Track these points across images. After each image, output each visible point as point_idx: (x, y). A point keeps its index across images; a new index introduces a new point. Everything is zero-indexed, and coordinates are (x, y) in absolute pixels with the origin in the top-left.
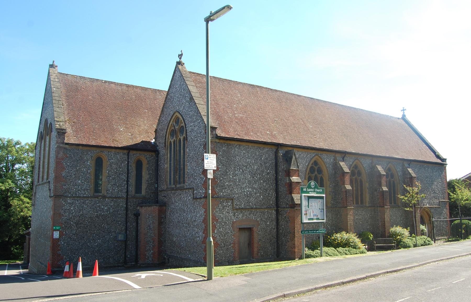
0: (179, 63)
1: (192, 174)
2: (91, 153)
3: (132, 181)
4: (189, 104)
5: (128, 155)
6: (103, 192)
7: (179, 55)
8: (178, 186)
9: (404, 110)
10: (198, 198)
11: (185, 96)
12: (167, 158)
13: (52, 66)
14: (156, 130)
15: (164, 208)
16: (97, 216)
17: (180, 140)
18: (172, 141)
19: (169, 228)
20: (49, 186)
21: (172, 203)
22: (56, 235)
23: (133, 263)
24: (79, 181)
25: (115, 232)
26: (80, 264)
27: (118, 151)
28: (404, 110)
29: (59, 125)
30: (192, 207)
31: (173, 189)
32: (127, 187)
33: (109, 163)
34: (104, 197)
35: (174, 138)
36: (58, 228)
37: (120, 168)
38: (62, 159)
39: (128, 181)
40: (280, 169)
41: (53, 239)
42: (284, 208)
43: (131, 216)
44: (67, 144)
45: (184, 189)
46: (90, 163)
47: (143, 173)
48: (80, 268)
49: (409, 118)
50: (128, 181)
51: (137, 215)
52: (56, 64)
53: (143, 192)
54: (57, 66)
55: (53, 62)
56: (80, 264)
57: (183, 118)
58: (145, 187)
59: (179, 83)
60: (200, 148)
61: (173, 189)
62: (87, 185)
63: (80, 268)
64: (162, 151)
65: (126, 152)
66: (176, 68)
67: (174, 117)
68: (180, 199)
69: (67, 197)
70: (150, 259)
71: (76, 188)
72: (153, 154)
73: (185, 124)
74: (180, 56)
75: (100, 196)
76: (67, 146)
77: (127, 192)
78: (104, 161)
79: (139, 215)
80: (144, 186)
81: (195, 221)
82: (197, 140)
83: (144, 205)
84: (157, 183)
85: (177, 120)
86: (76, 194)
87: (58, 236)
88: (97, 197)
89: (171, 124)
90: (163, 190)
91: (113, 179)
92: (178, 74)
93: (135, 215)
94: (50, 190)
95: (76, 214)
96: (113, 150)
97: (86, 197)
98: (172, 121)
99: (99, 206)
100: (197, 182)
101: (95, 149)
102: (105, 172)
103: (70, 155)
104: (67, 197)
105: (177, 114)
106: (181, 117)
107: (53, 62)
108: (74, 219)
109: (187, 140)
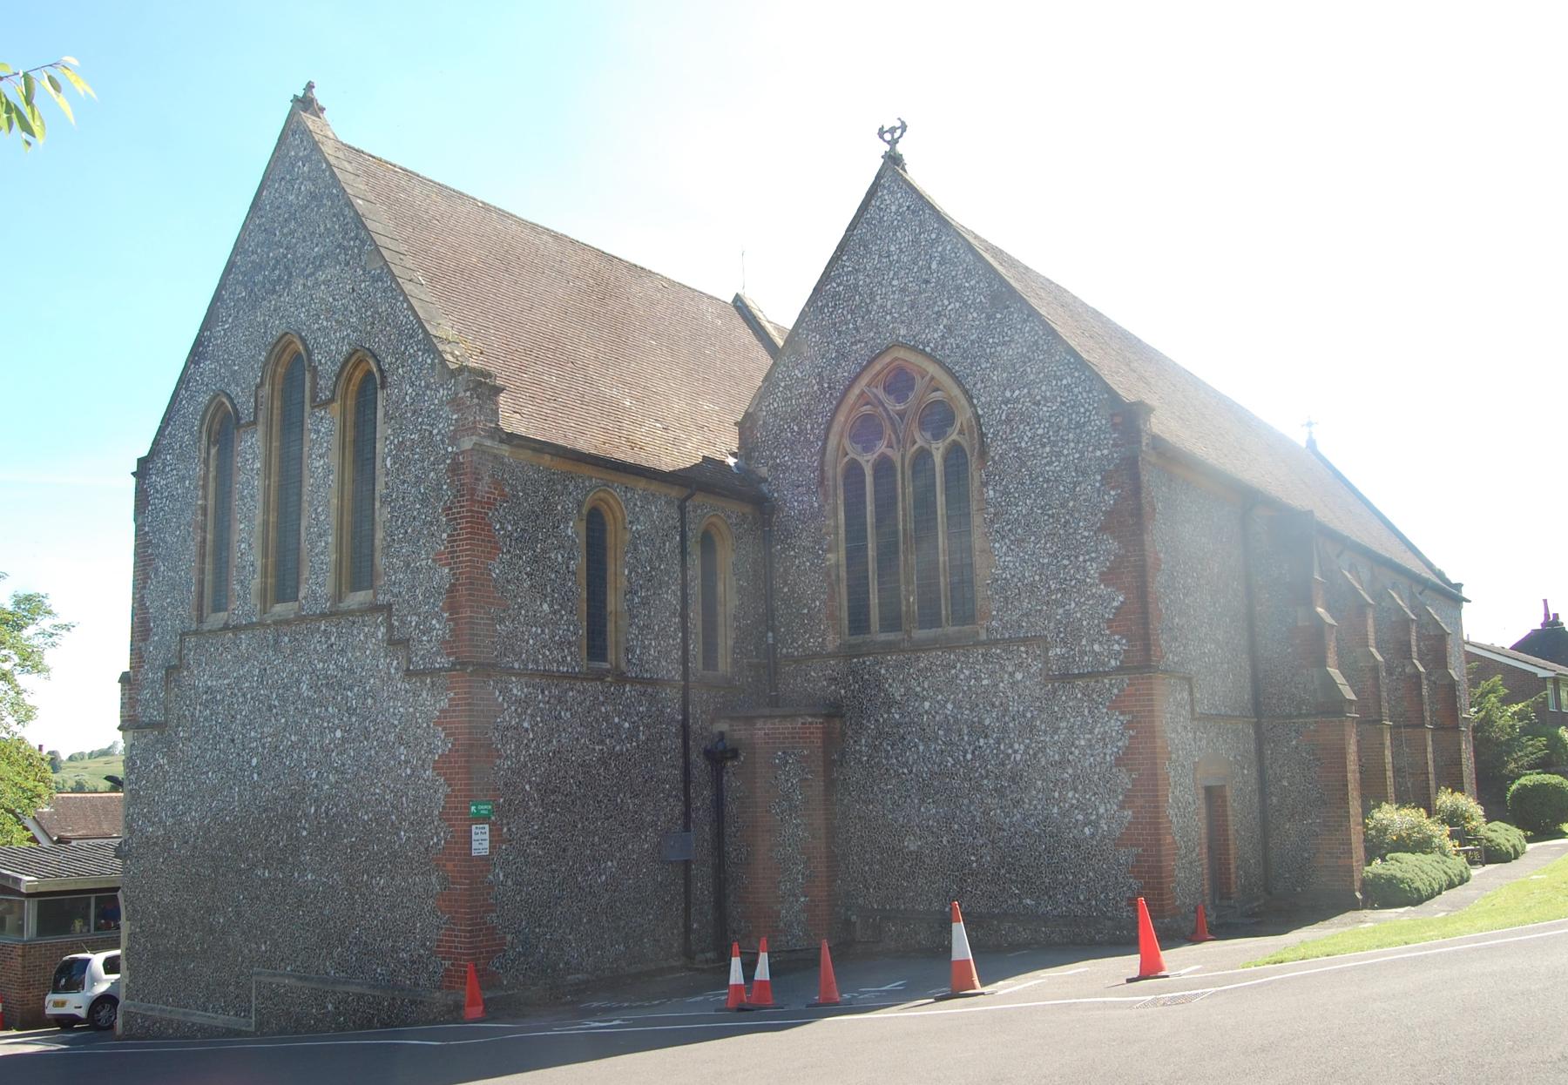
0: (893, 161)
2: (576, 487)
4: (989, 318)
5: (682, 509)
6: (611, 656)
7: (881, 133)
8: (919, 634)
9: (1310, 424)
10: (1080, 676)
12: (836, 527)
13: (306, 102)
14: (747, 415)
15: (837, 723)
16: (603, 762)
17: (924, 456)
18: (867, 461)
19: (867, 802)
20: (390, 627)
21: (889, 703)
22: (481, 841)
23: (710, 955)
24: (545, 606)
25: (654, 824)
26: (959, 931)
27: (654, 487)
28: (1310, 424)
29: (452, 354)
30: (1041, 710)
31: (889, 647)
32: (685, 640)
33: (628, 536)
34: (621, 678)
35: (881, 448)
36: (484, 809)
38: (490, 504)
39: (684, 616)
41: (473, 859)
42: (1289, 716)
43: (699, 762)
44: (511, 438)
45: (983, 644)
46: (574, 530)
47: (720, 587)
48: (961, 946)
49: (1321, 449)
52: (319, 95)
53: (724, 664)
54: (322, 110)
56: (959, 931)
57: (949, 371)
58: (730, 643)
59: (904, 236)
60: (1076, 484)
61: (889, 647)
62: (569, 623)
63: (961, 946)
64: (794, 501)
65: (675, 493)
66: (879, 177)
67: (877, 367)
69: (510, 671)
70: (797, 931)
71: (537, 635)
72: (748, 509)
73: (966, 392)
74: (892, 135)
75: (608, 671)
76: (505, 450)
77: (685, 660)
78: (610, 528)
79: (734, 754)
80: (726, 640)
81: (1061, 764)
82: (1059, 454)
83: (767, 711)
85: (899, 382)
86: (536, 662)
87: (486, 844)
88: (600, 677)
89: (856, 391)
90: (815, 655)
92: (892, 202)
93: (709, 754)
94: (397, 643)
95: (537, 748)
96: (642, 484)
97: (564, 676)
98: (864, 381)
99: (607, 718)
100: (1067, 614)
101: (587, 470)
103: (513, 487)
104: (510, 671)
105: (901, 353)
106: (932, 369)
108: (534, 770)
109: (983, 453)
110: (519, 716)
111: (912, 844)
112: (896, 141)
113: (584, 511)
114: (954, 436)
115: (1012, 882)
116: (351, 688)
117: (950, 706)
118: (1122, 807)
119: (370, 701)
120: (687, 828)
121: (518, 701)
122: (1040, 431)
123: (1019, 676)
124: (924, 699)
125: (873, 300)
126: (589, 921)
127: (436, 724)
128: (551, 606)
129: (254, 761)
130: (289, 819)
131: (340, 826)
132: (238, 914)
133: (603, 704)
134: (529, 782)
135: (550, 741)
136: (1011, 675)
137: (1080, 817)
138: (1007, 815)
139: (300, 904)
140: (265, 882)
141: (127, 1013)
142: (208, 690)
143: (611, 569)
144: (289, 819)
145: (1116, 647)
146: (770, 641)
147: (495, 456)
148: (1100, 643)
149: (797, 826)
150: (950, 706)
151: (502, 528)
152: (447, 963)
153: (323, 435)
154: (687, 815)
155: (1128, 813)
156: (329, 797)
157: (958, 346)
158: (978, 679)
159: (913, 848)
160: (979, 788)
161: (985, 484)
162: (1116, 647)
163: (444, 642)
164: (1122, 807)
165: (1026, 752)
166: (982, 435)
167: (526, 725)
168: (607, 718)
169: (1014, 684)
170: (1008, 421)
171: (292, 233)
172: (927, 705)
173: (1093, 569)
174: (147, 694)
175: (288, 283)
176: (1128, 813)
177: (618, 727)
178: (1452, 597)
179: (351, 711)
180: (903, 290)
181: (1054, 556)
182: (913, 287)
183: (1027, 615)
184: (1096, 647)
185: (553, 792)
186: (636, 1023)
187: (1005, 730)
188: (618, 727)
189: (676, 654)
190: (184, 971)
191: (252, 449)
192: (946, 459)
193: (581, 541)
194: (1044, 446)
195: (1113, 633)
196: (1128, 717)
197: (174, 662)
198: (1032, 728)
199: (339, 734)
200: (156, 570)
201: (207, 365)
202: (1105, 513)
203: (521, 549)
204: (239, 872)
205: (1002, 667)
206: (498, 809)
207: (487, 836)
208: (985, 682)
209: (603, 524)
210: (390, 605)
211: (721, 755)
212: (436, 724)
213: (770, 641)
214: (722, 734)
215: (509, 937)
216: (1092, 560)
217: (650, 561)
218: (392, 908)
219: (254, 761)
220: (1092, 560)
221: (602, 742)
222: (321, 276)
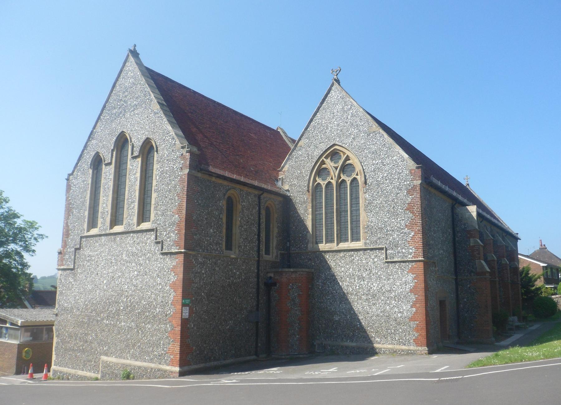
1: (381, 228)
3: (263, 235)
11: (357, 125)
24: (211, 230)
37: (252, 215)
39: (259, 236)
40: (458, 229)
43: (262, 286)
46: (223, 203)
50: (259, 236)
51: (270, 285)
55: (135, 46)
60: (398, 194)
65: (257, 192)
68: (352, 261)
71: (208, 241)
79: (274, 284)
84: (289, 241)
87: (187, 314)
91: (246, 230)
93: (266, 284)
99: (231, 270)
102: (237, 220)
107: (135, 46)
108: (205, 288)
109: (366, 183)
110: (201, 268)
111: (337, 318)
112: (337, 75)
113: (226, 197)
114: (355, 176)
115: (372, 332)
116: (141, 257)
117: (351, 270)
118: (412, 307)
119: (147, 262)
120: (257, 310)
121: (201, 263)
122: (385, 175)
123: (376, 260)
124: (342, 267)
125: (327, 128)
126: (223, 342)
127: (171, 271)
128: (213, 230)
129: (105, 282)
130: (116, 303)
131: (134, 306)
132: (96, 335)
133: (230, 265)
134: (203, 292)
135: (211, 278)
136: (373, 259)
137: (397, 310)
138: (370, 308)
139: (119, 333)
140: (107, 325)
141: (54, 370)
142: (89, 256)
143: (234, 218)
144: (116, 303)
145: (411, 251)
146: (288, 245)
147: (196, 177)
148: (405, 249)
149: (296, 310)
150: (351, 270)
151: (197, 202)
152: (172, 357)
153: (134, 168)
154: (258, 305)
155: (414, 309)
156: (131, 295)
157: (357, 145)
158: (361, 260)
159: (337, 319)
160: (361, 298)
161: (365, 193)
162: (411, 251)
163: (175, 241)
164: (412, 307)
165: (377, 287)
166: (365, 176)
167: (203, 272)
168: (231, 270)
169: (375, 262)
170: (374, 171)
171: (126, 96)
172: (343, 269)
173: (403, 223)
174: (67, 257)
175: (124, 115)
176: (414, 309)
177: (235, 274)
178: (515, 238)
179: (141, 265)
180: (338, 125)
181: (389, 218)
182: (342, 124)
183: (379, 238)
184: (404, 251)
185: (212, 296)
186: (242, 381)
187: (370, 278)
188: (235, 274)
189: (256, 249)
190: (76, 356)
191: (108, 174)
192: (351, 183)
193: (225, 208)
194: (386, 180)
195: (410, 246)
196: (415, 275)
197: (78, 246)
198: (380, 278)
199: (136, 273)
200: (73, 212)
201: (94, 142)
202: (408, 204)
203: (204, 210)
204: (98, 321)
205: (370, 256)
206: (192, 301)
207: (188, 311)
208: (364, 262)
209: (232, 202)
210: (156, 228)
211: (270, 285)
212: (171, 271)
213: (288, 245)
214: (271, 277)
215: (194, 348)
216: (403, 220)
217: (248, 216)
218: (152, 336)
219: (105, 282)
220: (403, 220)
221: (229, 279)
222: (136, 112)
